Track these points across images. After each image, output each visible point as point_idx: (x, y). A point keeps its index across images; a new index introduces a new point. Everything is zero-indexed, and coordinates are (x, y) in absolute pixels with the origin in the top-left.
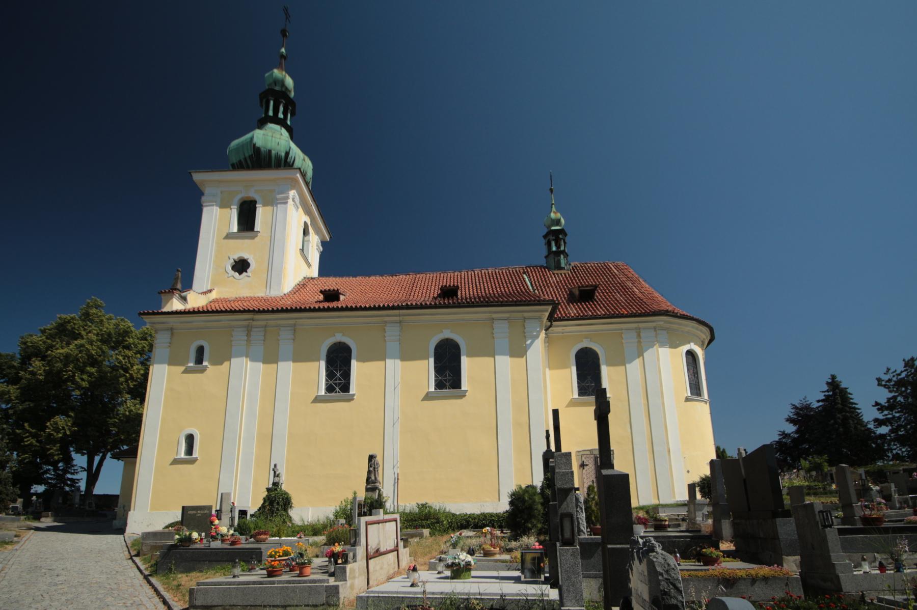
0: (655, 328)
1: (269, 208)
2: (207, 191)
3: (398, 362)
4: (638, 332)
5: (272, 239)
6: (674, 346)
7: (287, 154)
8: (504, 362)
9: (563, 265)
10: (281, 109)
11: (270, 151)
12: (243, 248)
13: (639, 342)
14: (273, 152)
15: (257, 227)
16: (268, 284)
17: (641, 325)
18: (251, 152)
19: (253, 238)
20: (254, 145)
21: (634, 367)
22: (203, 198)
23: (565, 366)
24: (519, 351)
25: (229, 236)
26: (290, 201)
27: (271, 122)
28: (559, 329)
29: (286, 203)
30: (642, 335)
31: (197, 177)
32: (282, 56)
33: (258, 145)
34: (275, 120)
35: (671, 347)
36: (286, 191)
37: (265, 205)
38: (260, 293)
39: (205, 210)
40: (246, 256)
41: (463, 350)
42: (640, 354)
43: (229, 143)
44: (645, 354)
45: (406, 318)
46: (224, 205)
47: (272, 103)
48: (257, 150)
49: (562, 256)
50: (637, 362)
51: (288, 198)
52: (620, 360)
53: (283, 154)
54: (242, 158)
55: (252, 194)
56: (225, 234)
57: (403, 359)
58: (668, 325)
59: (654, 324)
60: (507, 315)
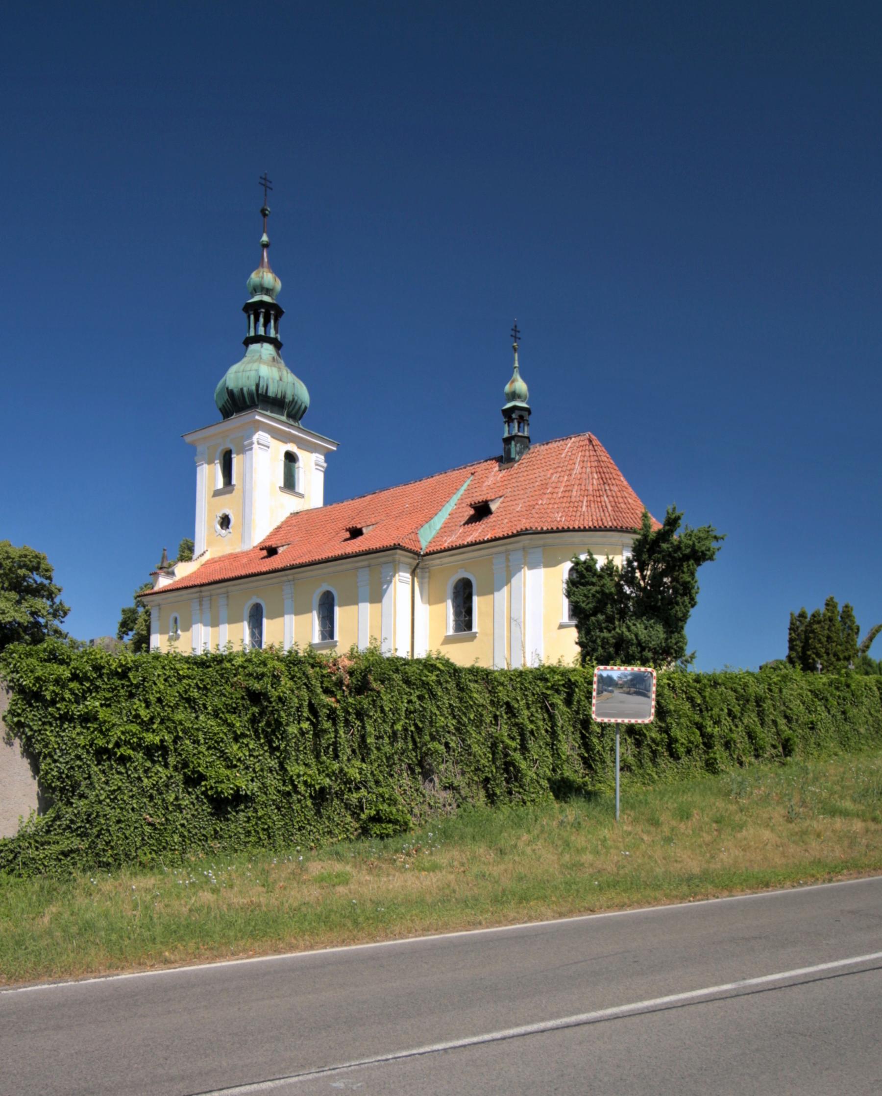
0: (524, 548)
1: (241, 456)
2: (199, 449)
3: (293, 617)
4: (507, 552)
5: (244, 492)
6: (551, 562)
7: (258, 386)
8: (366, 608)
9: (513, 456)
10: (262, 320)
11: (242, 390)
12: (227, 506)
13: (508, 567)
14: (245, 390)
15: (234, 482)
16: (242, 538)
17: (509, 547)
18: (226, 396)
19: (231, 492)
20: (227, 389)
21: (502, 596)
22: (196, 459)
23: (442, 600)
24: (377, 597)
25: (217, 493)
26: (255, 446)
27: (252, 343)
28: (438, 562)
29: (251, 449)
30: (510, 557)
31: (188, 439)
32: (266, 246)
33: (230, 388)
34: (258, 339)
35: (546, 566)
36: (250, 437)
37: (238, 454)
38: (238, 550)
39: (198, 469)
40: (227, 511)
41: (336, 601)
42: (508, 581)
43: (216, 386)
44: (514, 581)
45: (296, 576)
46: (210, 462)
47: (252, 317)
48: (230, 393)
49: (513, 443)
50: (505, 589)
51: (252, 443)
52: (490, 589)
53: (254, 388)
54: (223, 402)
55: (231, 446)
56: (212, 493)
57: (297, 613)
58: (541, 542)
59: (520, 545)
60: (366, 563)
